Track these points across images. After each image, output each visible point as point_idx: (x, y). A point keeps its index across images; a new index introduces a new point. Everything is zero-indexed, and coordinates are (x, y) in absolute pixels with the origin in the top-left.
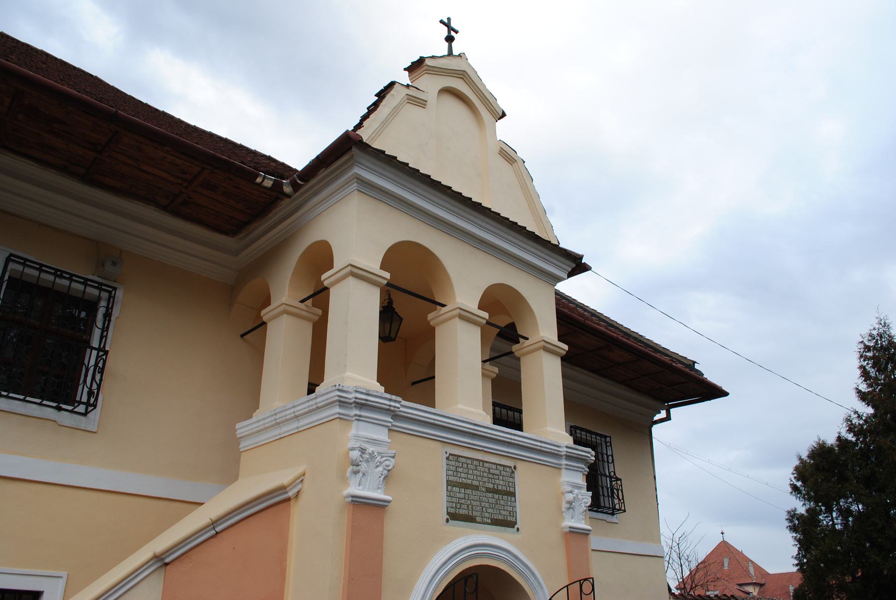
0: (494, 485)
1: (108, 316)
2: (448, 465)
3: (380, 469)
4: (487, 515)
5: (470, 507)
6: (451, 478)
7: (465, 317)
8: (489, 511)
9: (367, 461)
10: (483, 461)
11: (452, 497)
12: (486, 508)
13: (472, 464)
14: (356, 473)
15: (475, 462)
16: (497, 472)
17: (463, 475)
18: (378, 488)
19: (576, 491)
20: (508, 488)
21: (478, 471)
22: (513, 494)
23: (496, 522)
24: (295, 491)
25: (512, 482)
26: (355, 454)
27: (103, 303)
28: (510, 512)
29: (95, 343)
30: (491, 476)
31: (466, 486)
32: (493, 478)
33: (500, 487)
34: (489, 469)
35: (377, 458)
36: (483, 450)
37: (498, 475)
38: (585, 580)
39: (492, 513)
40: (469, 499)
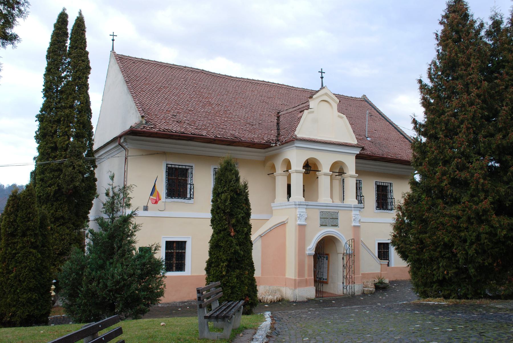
14: (299, 219)
19: (356, 216)
22: (338, 219)
23: (332, 226)
26: (298, 216)
31: (325, 218)
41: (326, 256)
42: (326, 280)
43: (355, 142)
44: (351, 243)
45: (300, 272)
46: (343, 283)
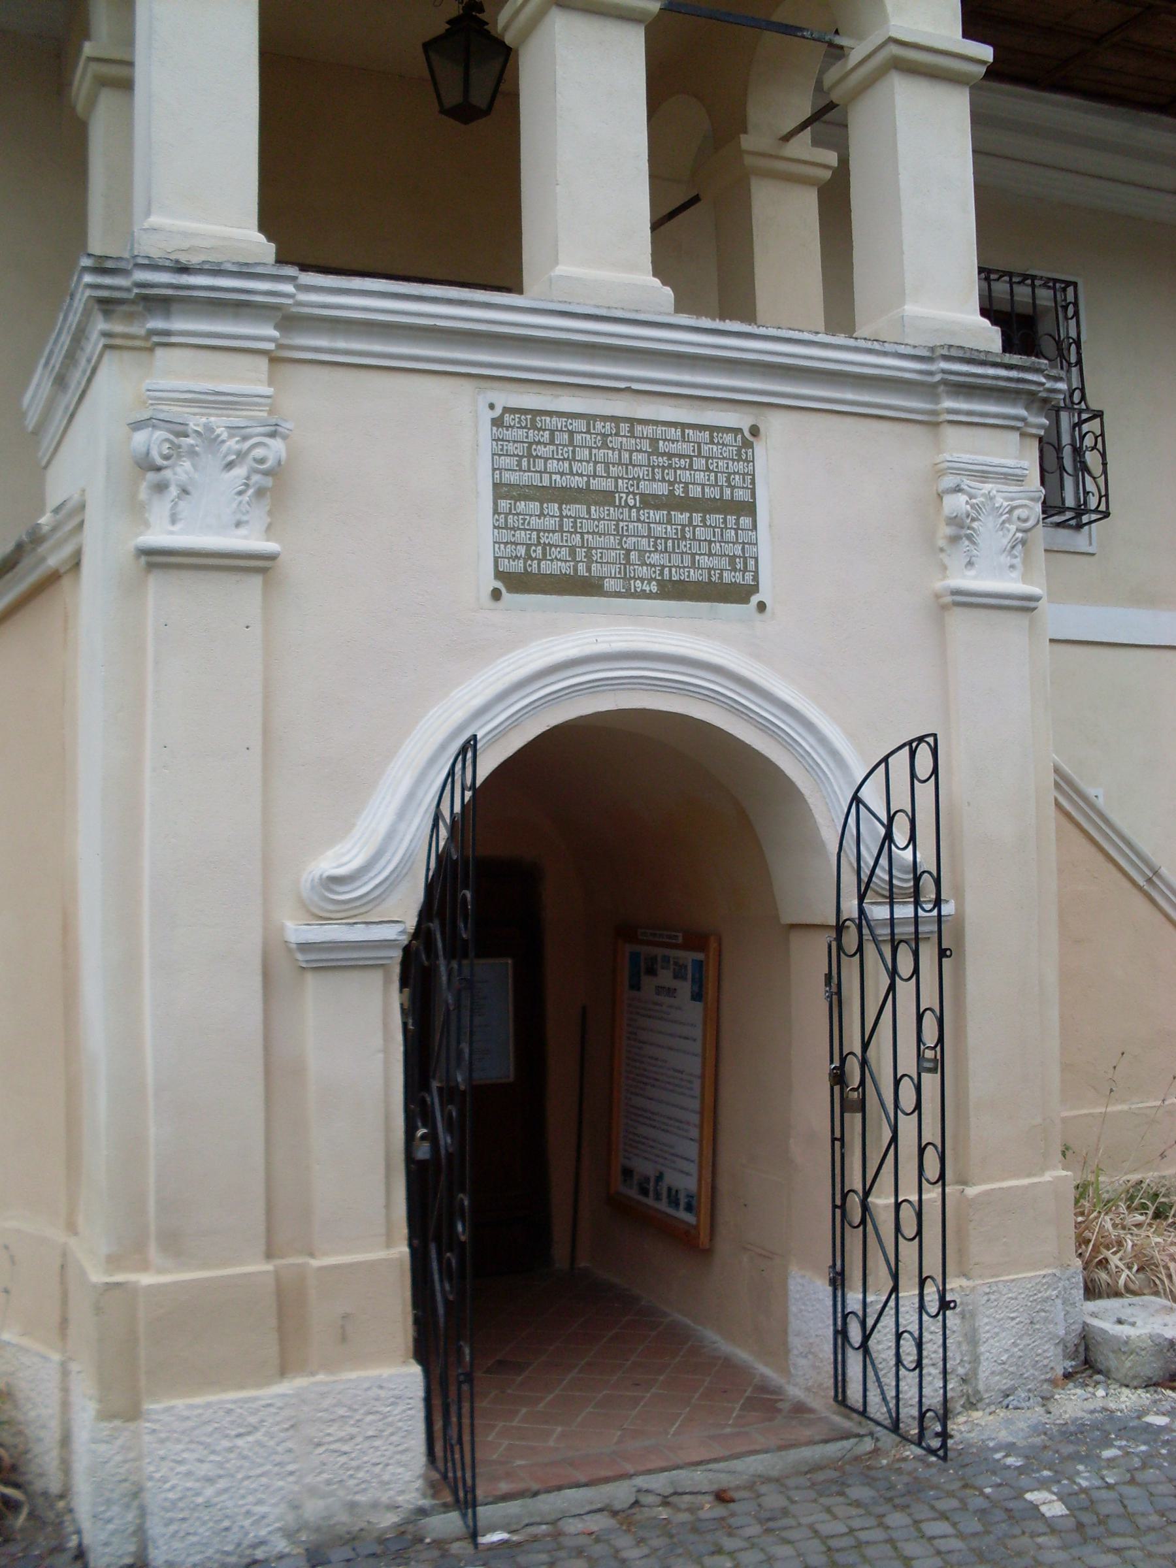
0: (671, 484)
2: (499, 440)
3: (240, 472)
4: (644, 571)
5: (581, 553)
6: (509, 477)
8: (655, 558)
9: (192, 453)
10: (632, 421)
11: (513, 529)
12: (642, 553)
13: (588, 432)
14: (161, 488)
15: (599, 425)
16: (686, 448)
17: (553, 465)
18: (238, 524)
20: (728, 491)
21: (613, 449)
22: (749, 509)
24: (67, 550)
25: (744, 474)
28: (732, 559)
30: (662, 460)
31: (565, 496)
32: (670, 466)
33: (695, 492)
34: (654, 441)
35: (223, 442)
36: (628, 389)
37: (691, 457)
38: (921, 739)
39: (663, 567)
40: (576, 532)
41: (689, 957)
42: (689, 1208)
44: (900, 800)
46: (838, 1281)
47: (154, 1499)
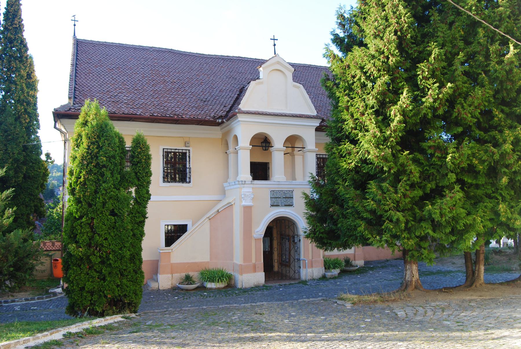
1: (189, 157)
7: (279, 150)
22: (293, 198)
23: (286, 206)
27: (188, 154)
29: (188, 167)
31: (276, 198)
43: (315, 113)
45: (247, 256)
47: (243, 282)
